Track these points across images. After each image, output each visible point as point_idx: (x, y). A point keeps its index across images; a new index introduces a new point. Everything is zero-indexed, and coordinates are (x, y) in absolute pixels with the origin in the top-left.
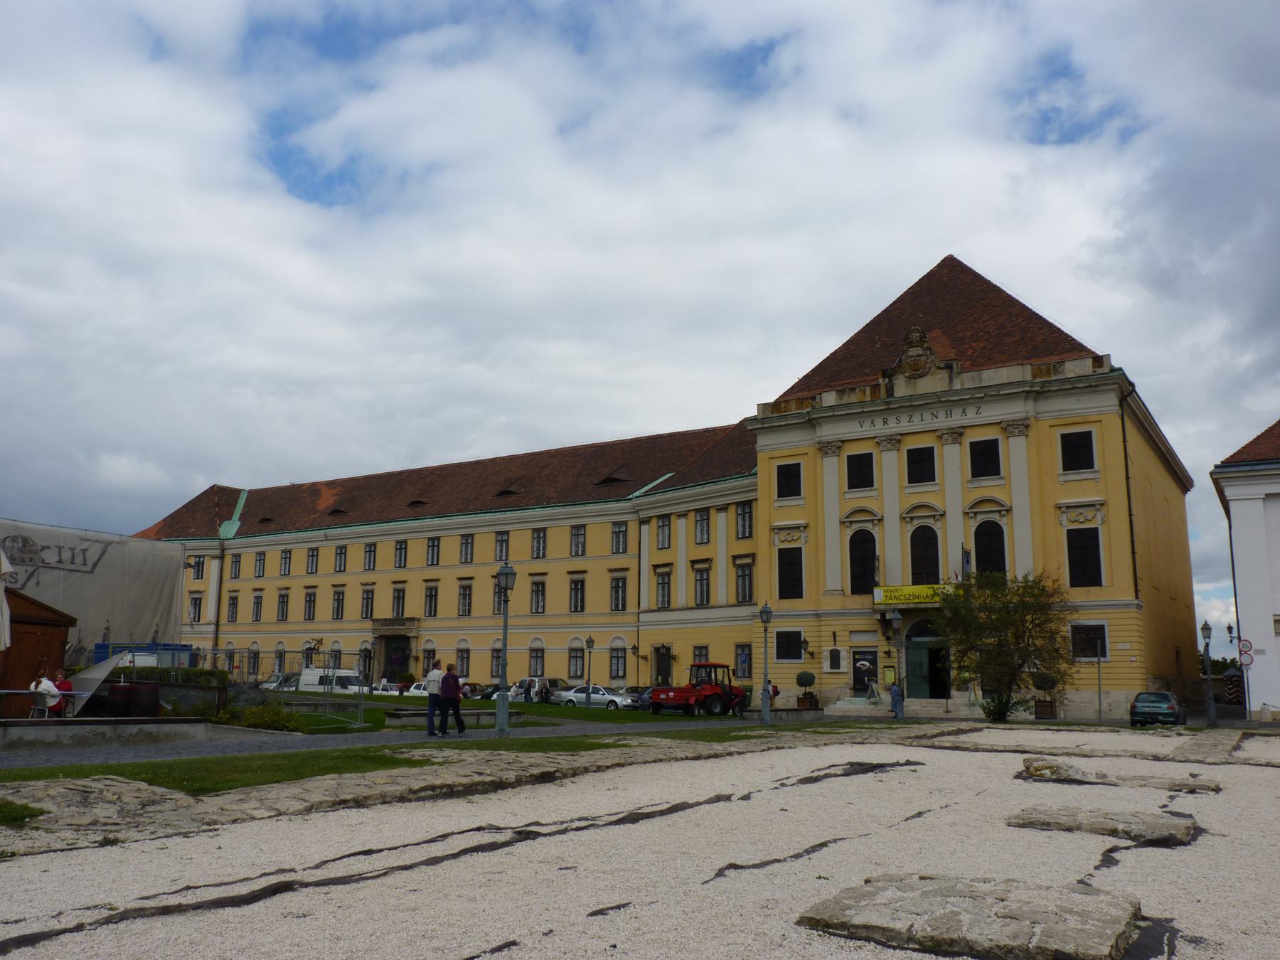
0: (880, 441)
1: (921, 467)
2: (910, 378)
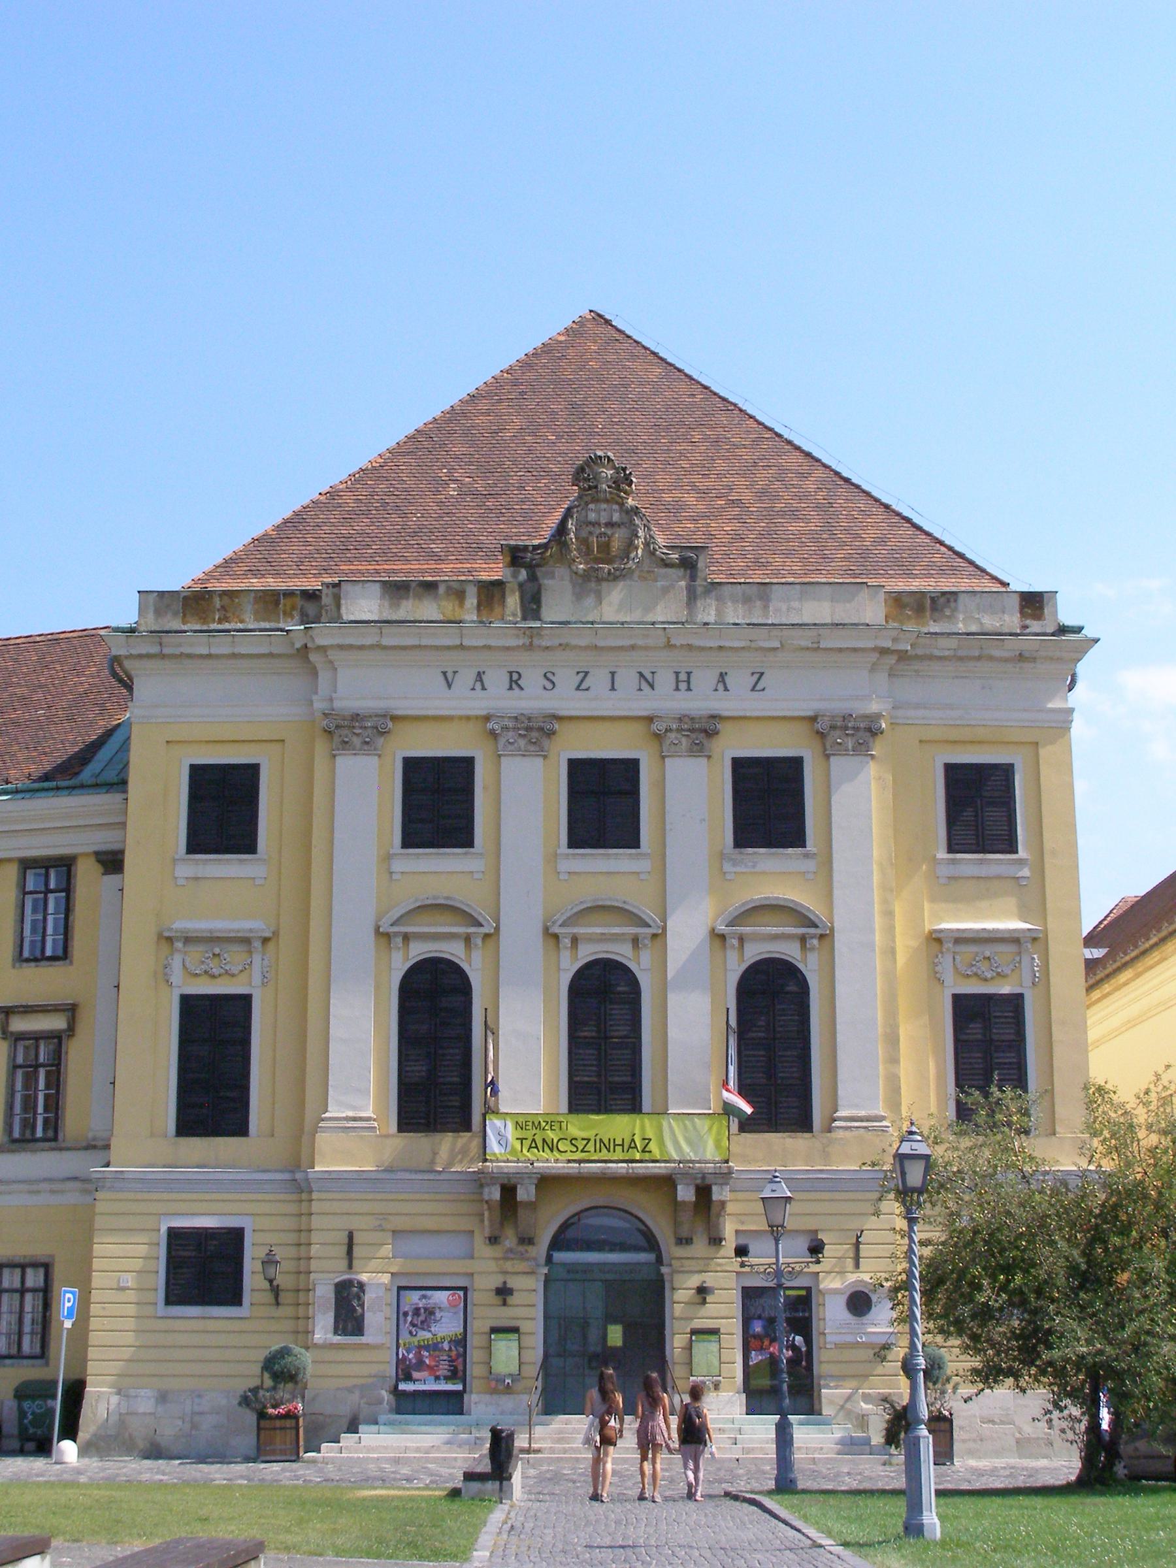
0: (491, 728)
1: (603, 805)
2: (586, 576)
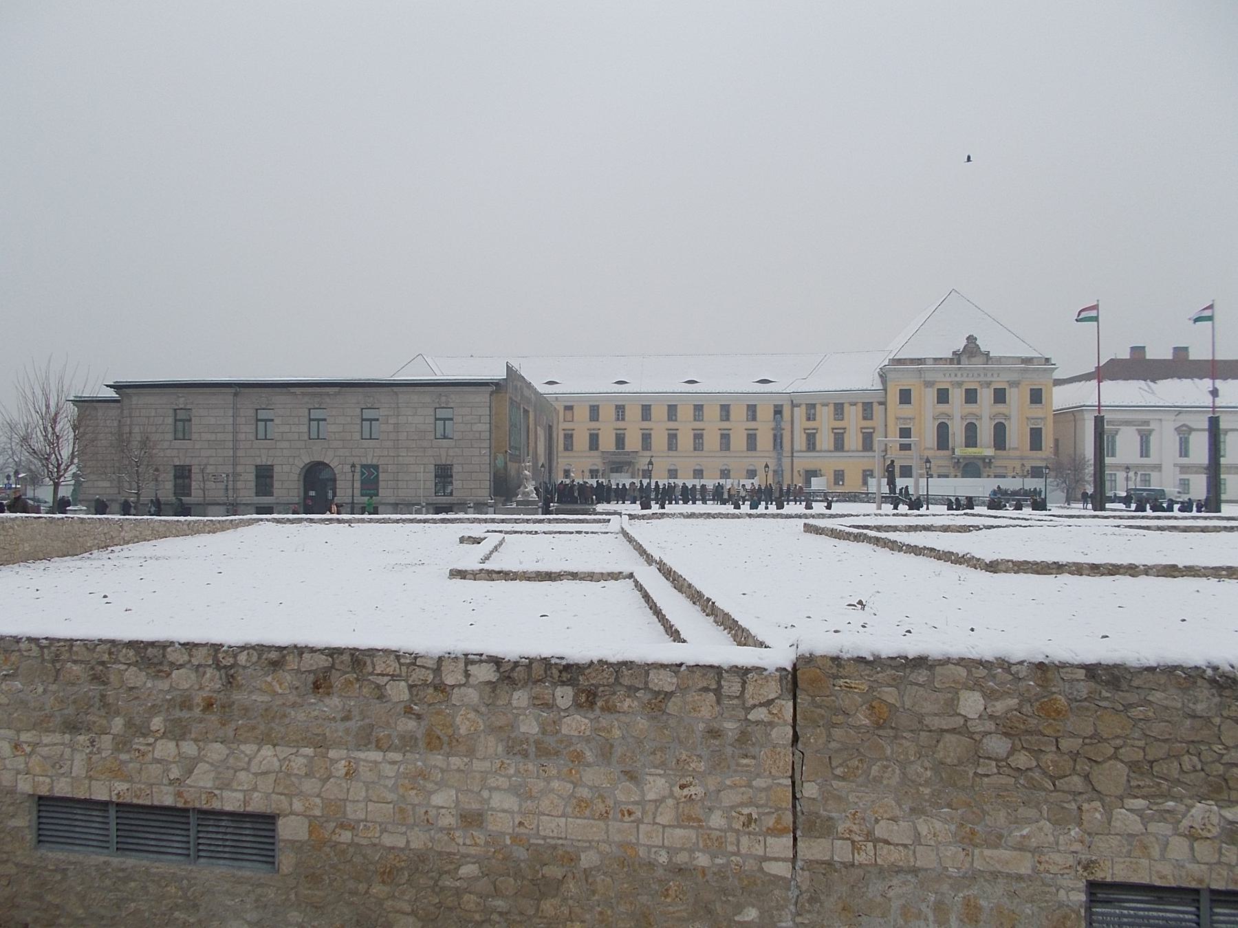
1: (971, 396)
